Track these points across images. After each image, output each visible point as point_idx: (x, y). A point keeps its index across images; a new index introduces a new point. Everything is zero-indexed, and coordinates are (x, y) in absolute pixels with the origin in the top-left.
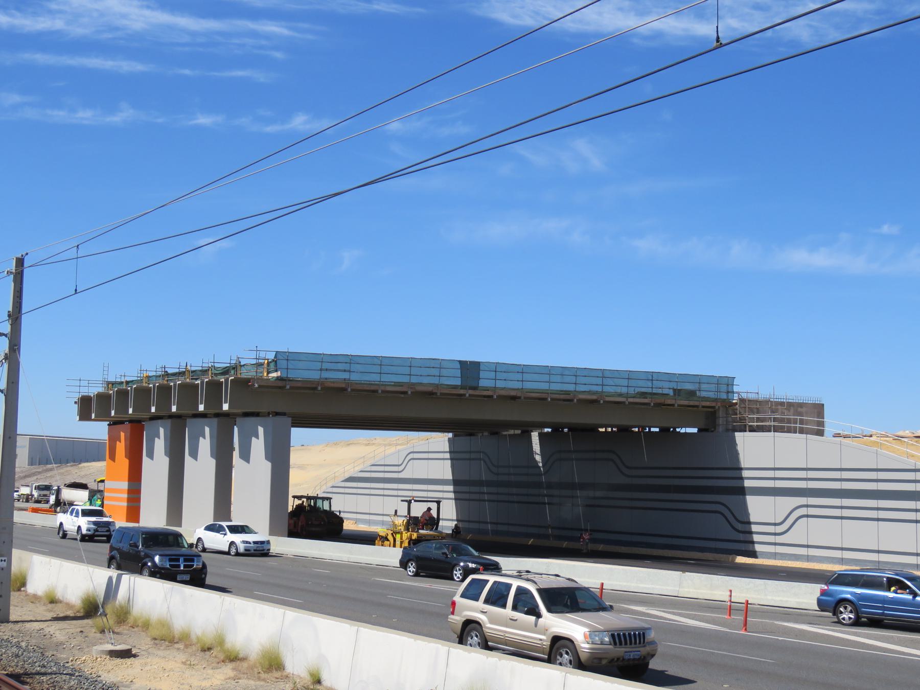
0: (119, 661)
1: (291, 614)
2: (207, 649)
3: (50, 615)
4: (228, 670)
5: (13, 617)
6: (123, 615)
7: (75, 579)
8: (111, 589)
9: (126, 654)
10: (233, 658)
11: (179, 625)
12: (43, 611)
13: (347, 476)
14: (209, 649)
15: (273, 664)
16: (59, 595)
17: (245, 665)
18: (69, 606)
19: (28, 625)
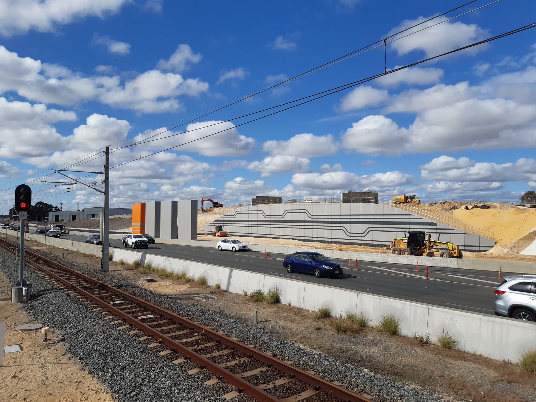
0: (150, 283)
1: (209, 266)
2: (179, 278)
3: (122, 269)
4: (188, 285)
5: (110, 270)
6: (149, 267)
7: (131, 257)
8: (143, 258)
9: (152, 281)
10: (189, 281)
11: (169, 270)
12: (119, 267)
13: (215, 219)
14: (180, 278)
15: (203, 282)
16: (125, 261)
17: (194, 283)
18: (128, 265)
19: (116, 272)
